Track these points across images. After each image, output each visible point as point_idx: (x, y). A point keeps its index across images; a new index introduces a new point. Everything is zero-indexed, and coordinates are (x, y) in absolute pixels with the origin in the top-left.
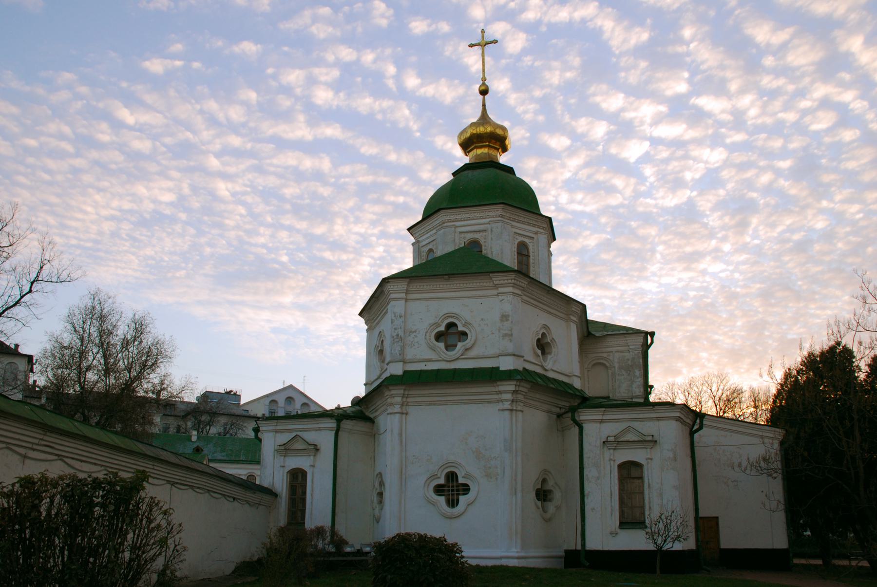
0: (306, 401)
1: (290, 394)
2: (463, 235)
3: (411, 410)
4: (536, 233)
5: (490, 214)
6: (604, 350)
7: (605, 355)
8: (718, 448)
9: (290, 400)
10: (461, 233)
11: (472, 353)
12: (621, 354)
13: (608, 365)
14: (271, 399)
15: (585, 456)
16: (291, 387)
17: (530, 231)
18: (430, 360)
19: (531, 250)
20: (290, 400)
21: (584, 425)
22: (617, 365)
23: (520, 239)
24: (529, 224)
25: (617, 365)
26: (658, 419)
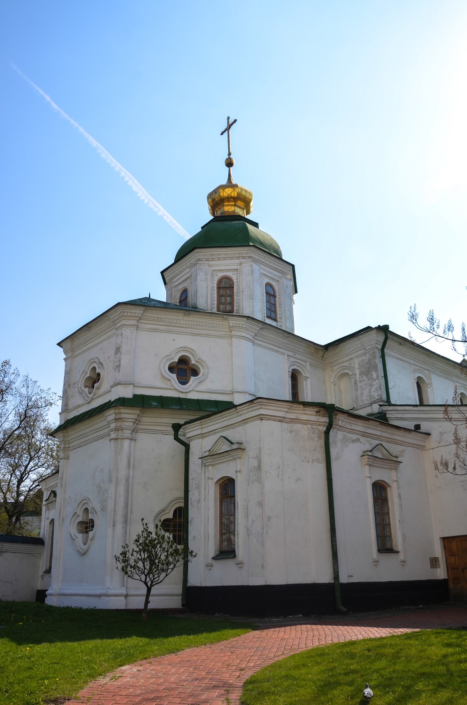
6: (341, 361)
7: (346, 364)
12: (361, 359)
13: (351, 373)
15: (190, 477)
19: (235, 281)
22: (357, 372)
23: (221, 275)
24: (231, 258)
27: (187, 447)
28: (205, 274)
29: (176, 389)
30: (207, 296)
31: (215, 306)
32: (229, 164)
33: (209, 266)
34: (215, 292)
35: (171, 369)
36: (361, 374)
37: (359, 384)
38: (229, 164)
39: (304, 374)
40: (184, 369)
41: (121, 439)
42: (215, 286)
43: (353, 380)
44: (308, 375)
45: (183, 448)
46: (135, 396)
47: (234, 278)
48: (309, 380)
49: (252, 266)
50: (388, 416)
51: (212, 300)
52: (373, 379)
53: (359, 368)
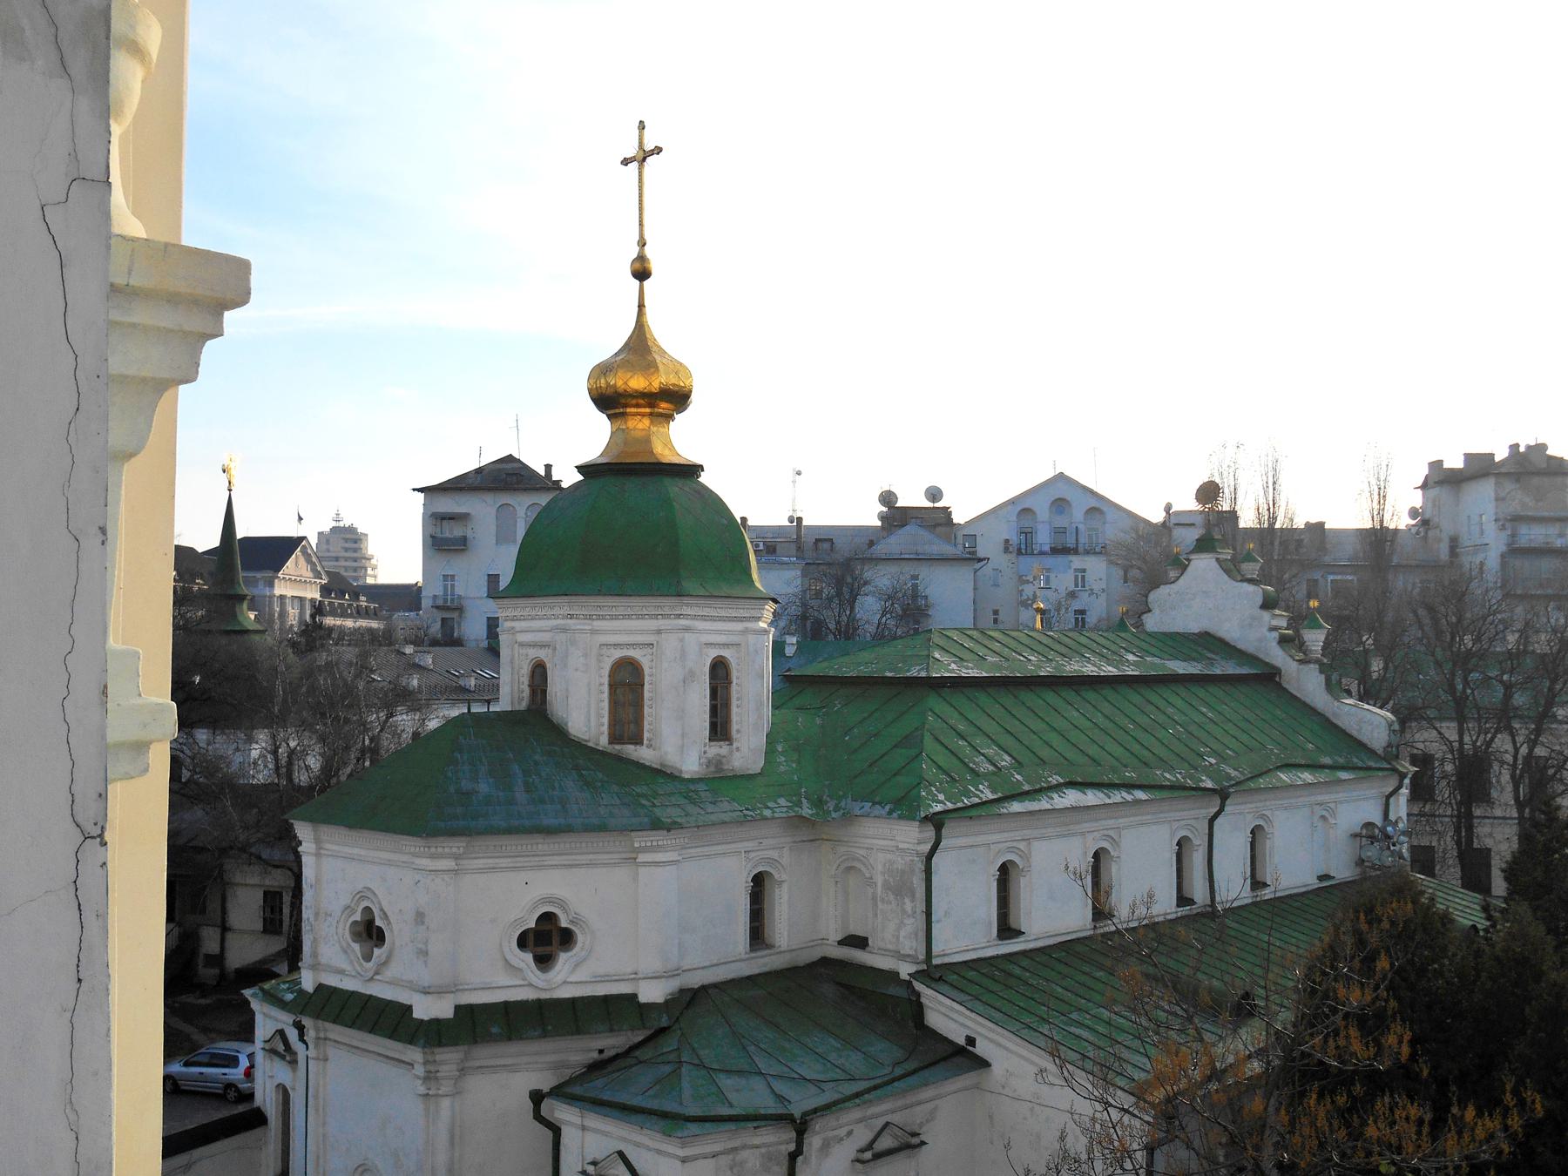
0: (1097, 505)
1: (1061, 494)
2: (523, 651)
3: (332, 1052)
4: (659, 632)
5: (556, 611)
8: (1037, 1108)
9: (1060, 505)
10: (522, 645)
11: (391, 972)
12: (889, 856)
14: (1021, 508)
16: (1061, 478)
17: (642, 632)
18: (341, 972)
19: (647, 671)
20: (1060, 505)
21: (563, 1128)
22: (879, 880)
23: (618, 654)
25: (879, 880)
26: (659, 1152)
27: (556, 1131)
28: (585, 655)
29: (530, 985)
30: (589, 705)
31: (605, 728)
32: (641, 273)
33: (594, 632)
34: (606, 695)
35: (523, 942)
36: (886, 886)
37: (880, 905)
38: (641, 273)
39: (776, 876)
40: (546, 938)
41: (437, 1095)
42: (606, 680)
43: (870, 891)
44: (784, 877)
45: (550, 1134)
46: (458, 1008)
47: (646, 664)
48: (785, 887)
49: (682, 640)
50: (923, 1000)
51: (600, 716)
52: (904, 911)
53: (883, 873)
